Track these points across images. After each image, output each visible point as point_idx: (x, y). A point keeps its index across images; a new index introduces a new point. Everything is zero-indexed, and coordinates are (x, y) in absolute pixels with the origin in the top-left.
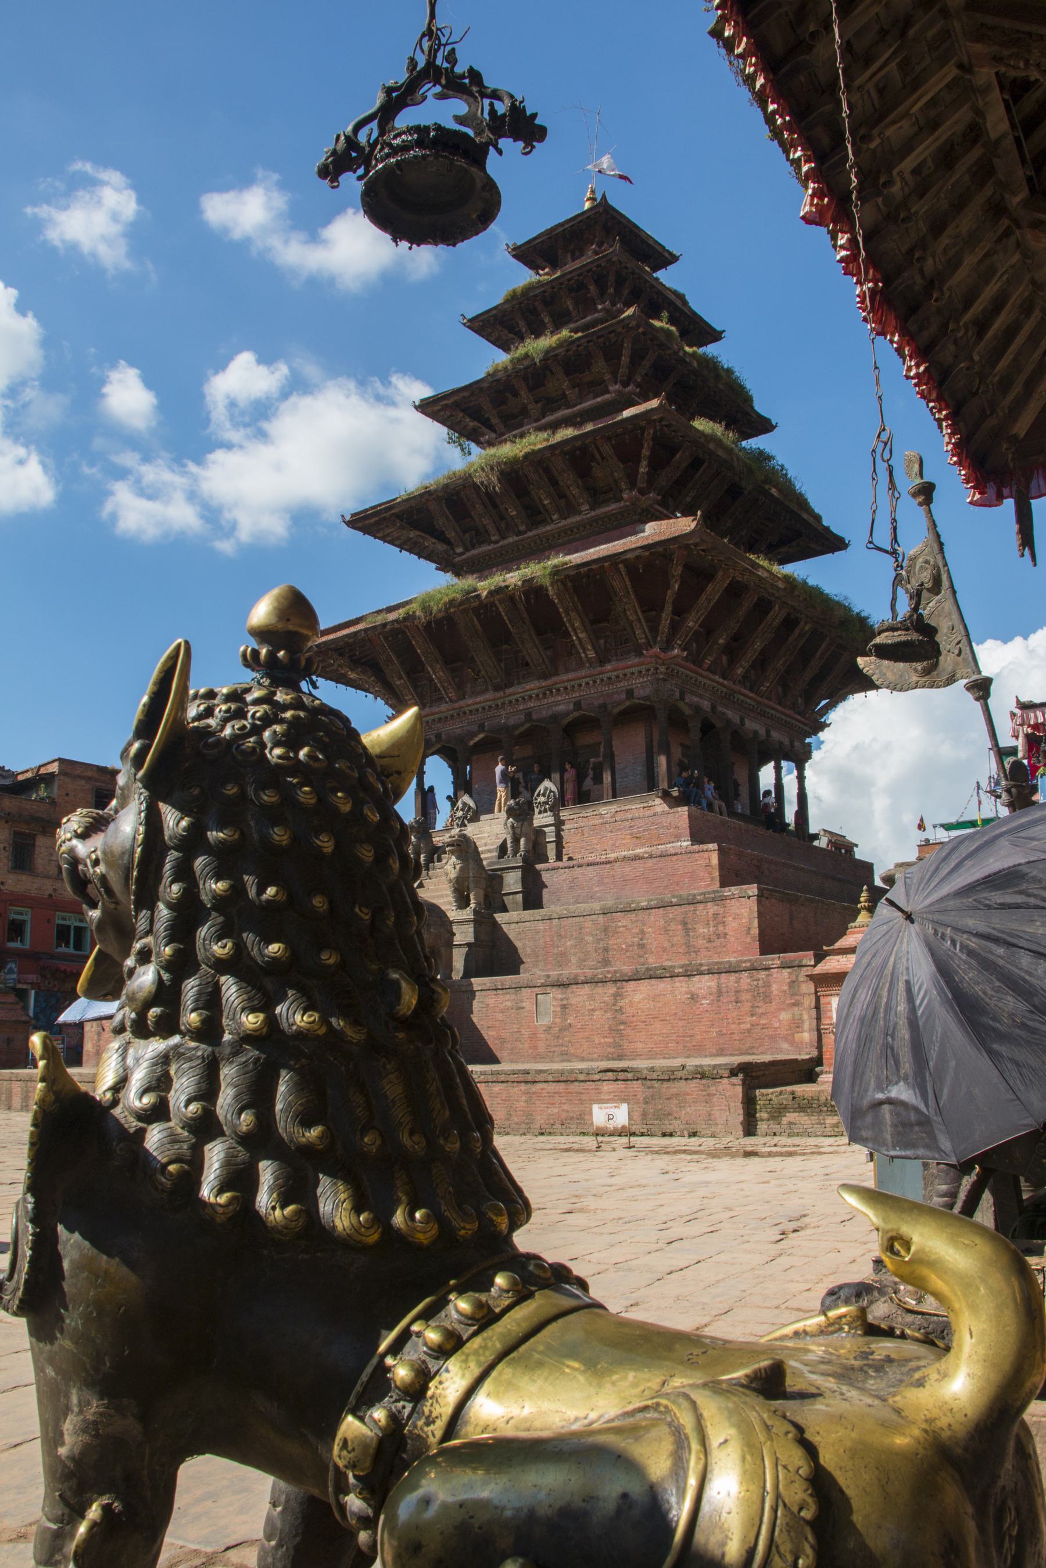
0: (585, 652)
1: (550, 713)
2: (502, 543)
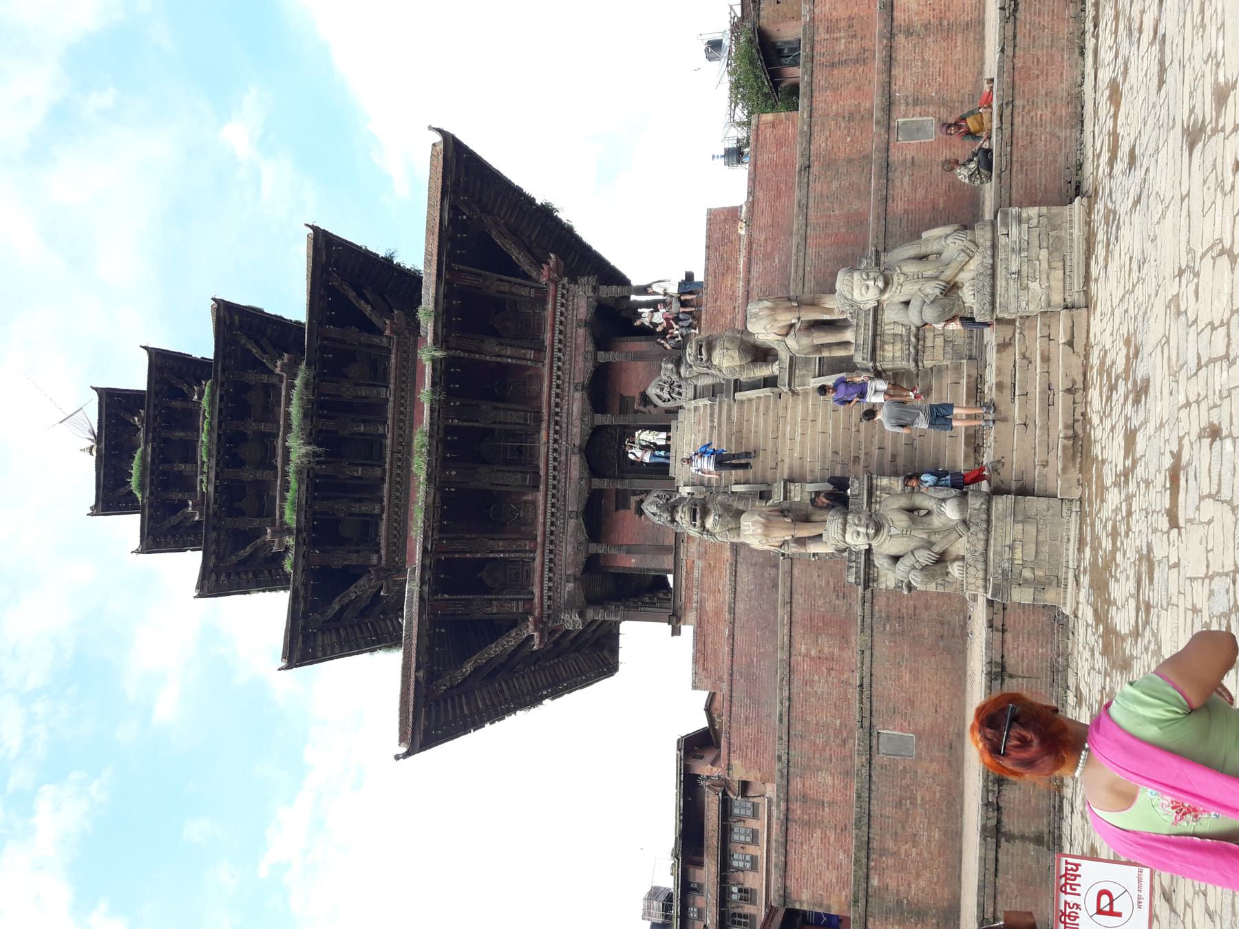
1: (578, 423)
2: (385, 503)
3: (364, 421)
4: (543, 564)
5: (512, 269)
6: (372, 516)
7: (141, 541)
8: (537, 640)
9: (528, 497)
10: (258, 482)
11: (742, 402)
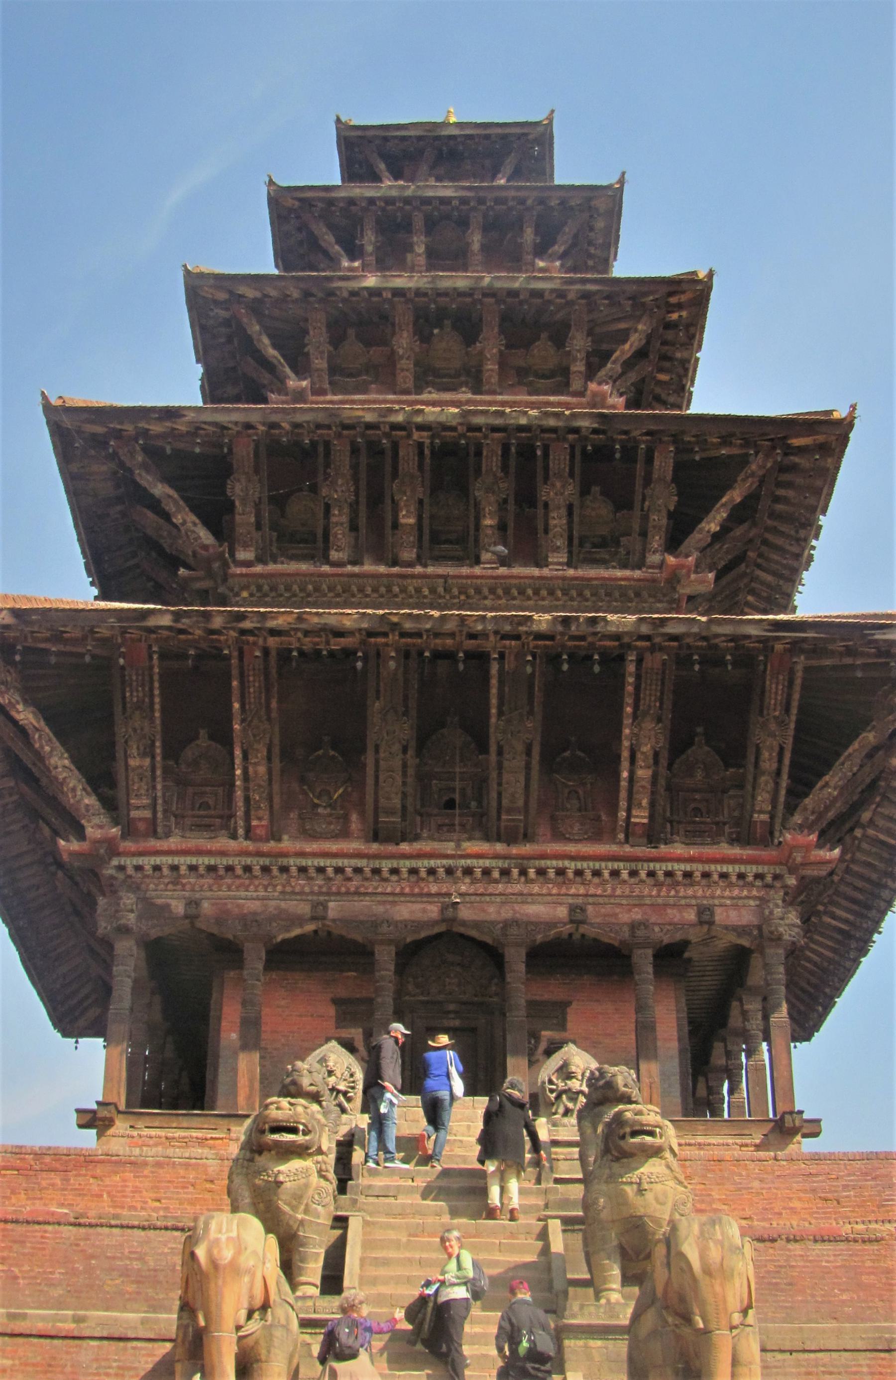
0: (629, 810)
1: (506, 913)
2: (349, 568)
3: (502, 527)
4: (223, 853)
5: (804, 777)
6: (326, 549)
7: (289, 189)
10: (392, 359)
11: (543, 1235)
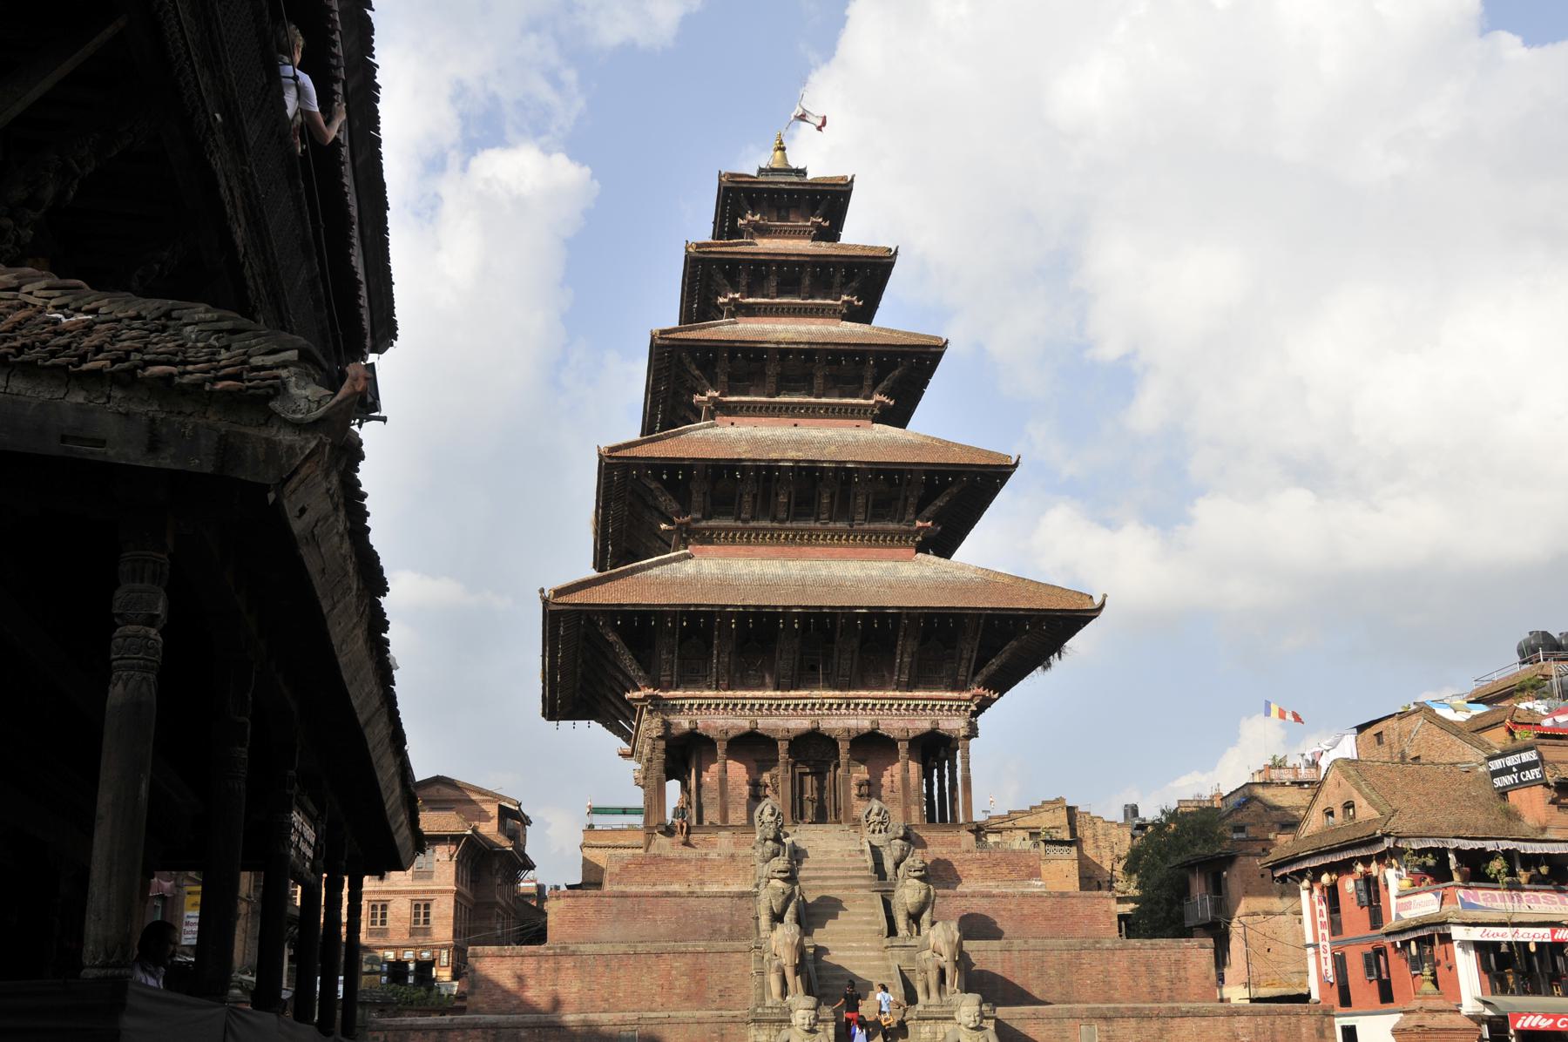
3: (832, 503)
8: (636, 695)
9: (768, 680)
